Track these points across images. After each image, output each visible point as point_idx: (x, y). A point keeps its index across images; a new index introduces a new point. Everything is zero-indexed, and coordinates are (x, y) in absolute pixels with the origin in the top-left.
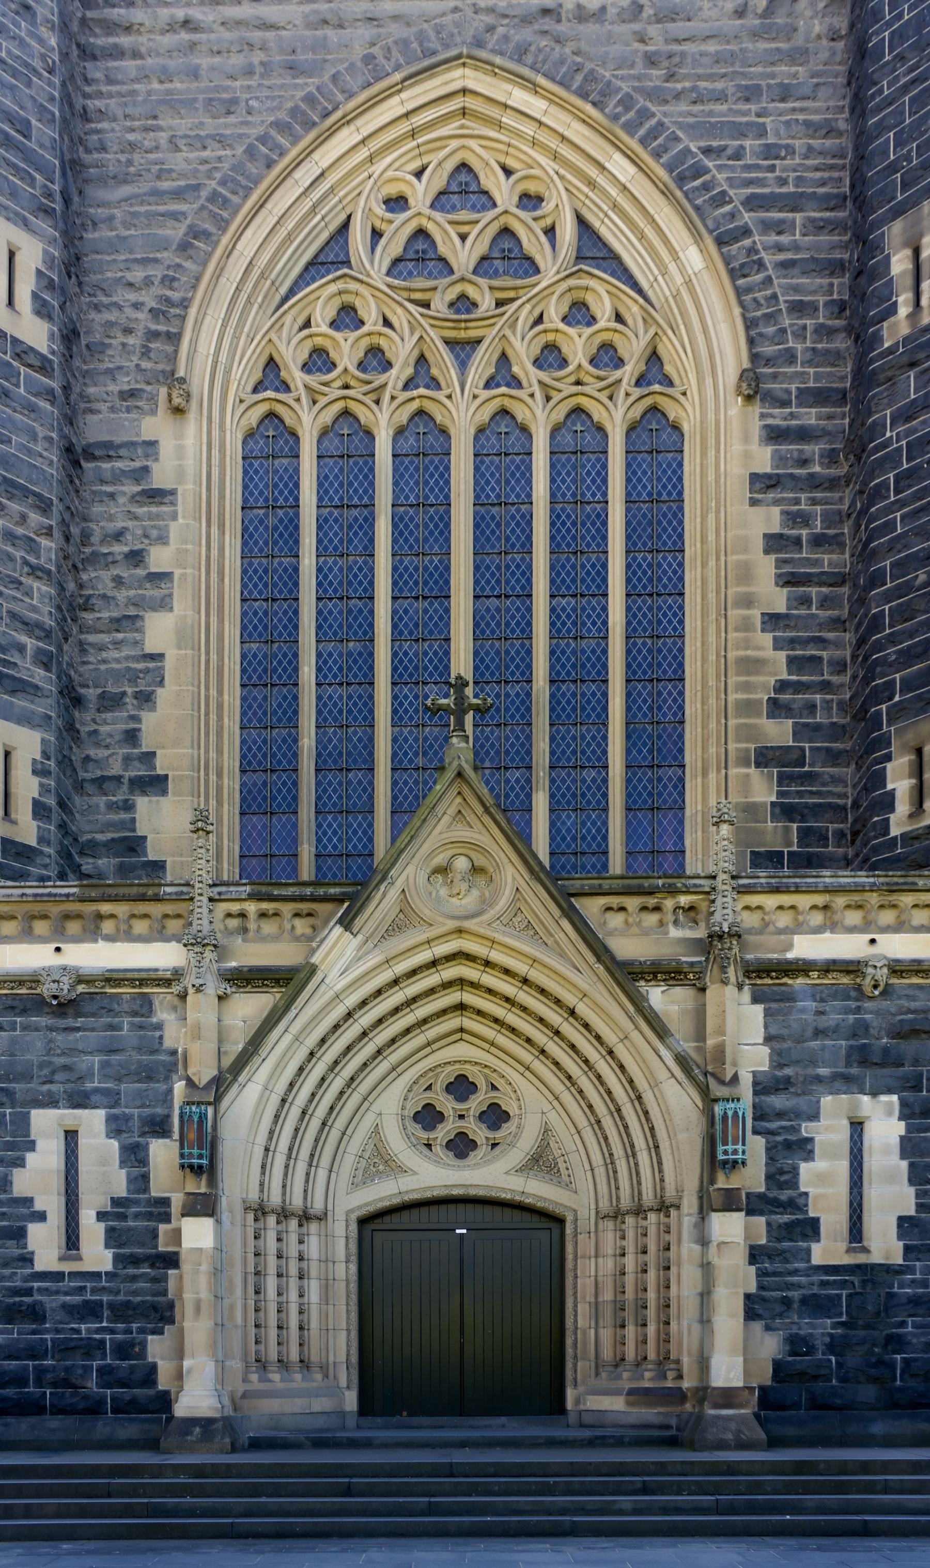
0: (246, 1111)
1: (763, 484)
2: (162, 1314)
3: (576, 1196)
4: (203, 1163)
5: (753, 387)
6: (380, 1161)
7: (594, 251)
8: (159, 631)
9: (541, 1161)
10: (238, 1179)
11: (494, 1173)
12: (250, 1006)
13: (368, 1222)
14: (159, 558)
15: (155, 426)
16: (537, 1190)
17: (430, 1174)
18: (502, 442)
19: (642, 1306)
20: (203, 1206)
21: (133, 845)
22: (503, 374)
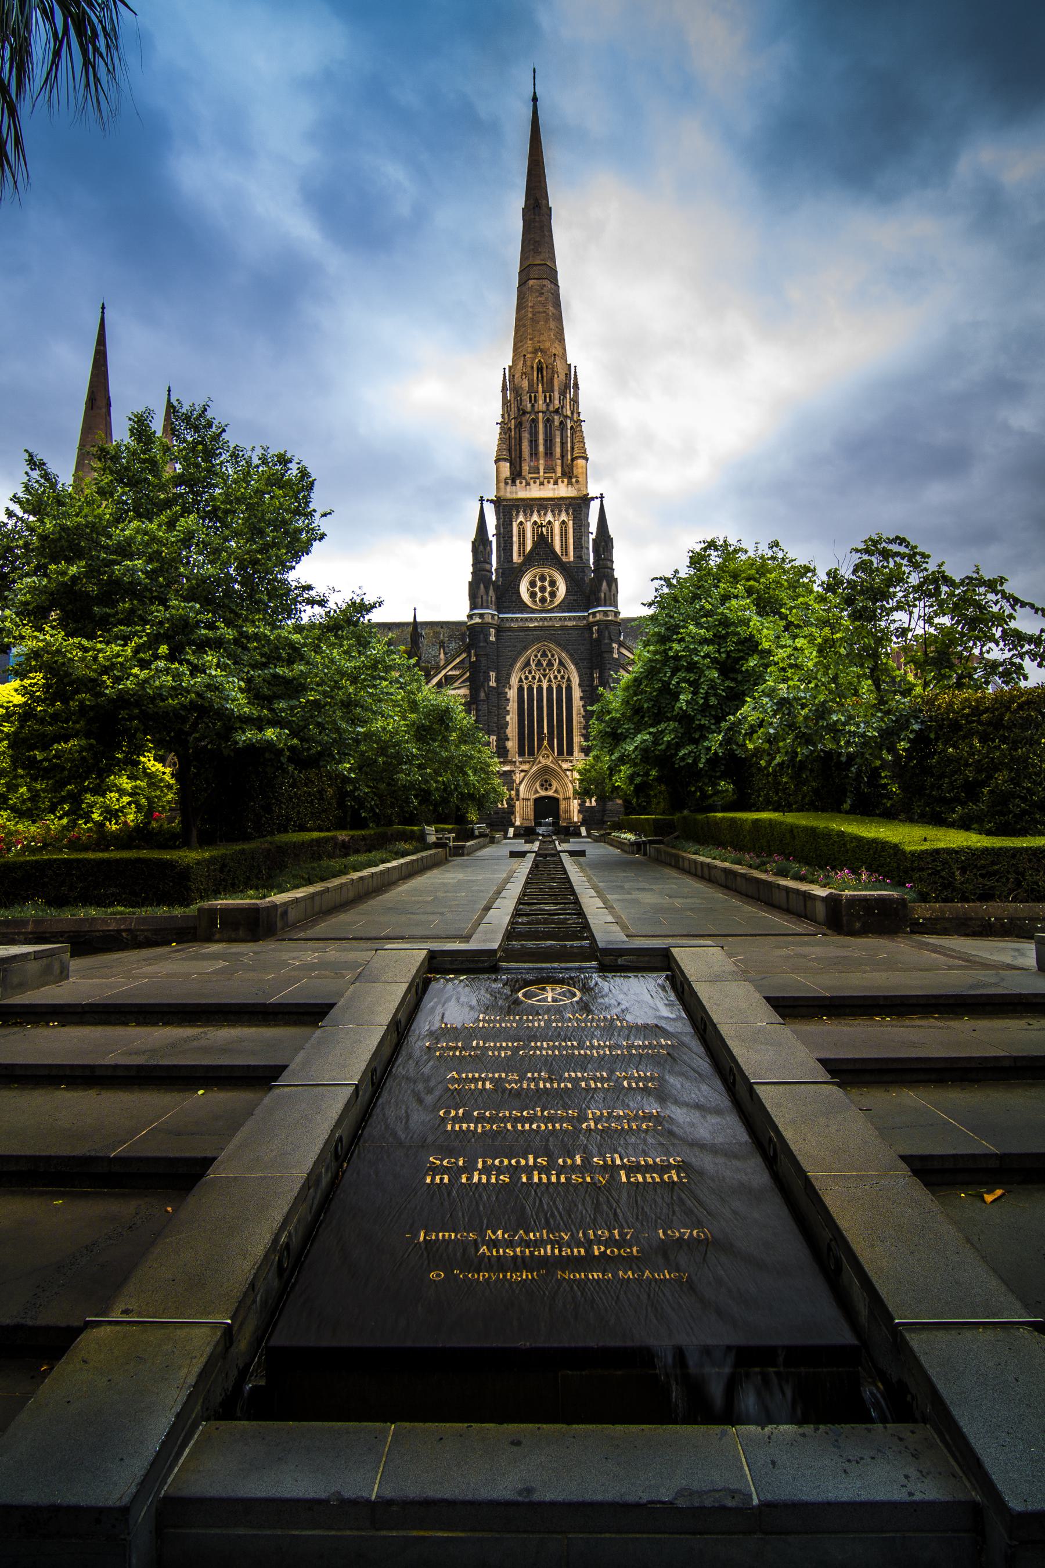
0: (522, 788)
1: (581, 698)
2: (513, 813)
3: (561, 796)
4: (518, 795)
5: (580, 685)
6: (537, 792)
7: (561, 663)
8: (508, 718)
9: (556, 791)
10: (522, 795)
11: (550, 793)
12: (523, 774)
13: (536, 800)
14: (508, 708)
15: (507, 690)
16: (556, 795)
17: (543, 793)
18: (550, 689)
19: (568, 811)
20: (518, 800)
21: (505, 747)
22: (550, 680)
